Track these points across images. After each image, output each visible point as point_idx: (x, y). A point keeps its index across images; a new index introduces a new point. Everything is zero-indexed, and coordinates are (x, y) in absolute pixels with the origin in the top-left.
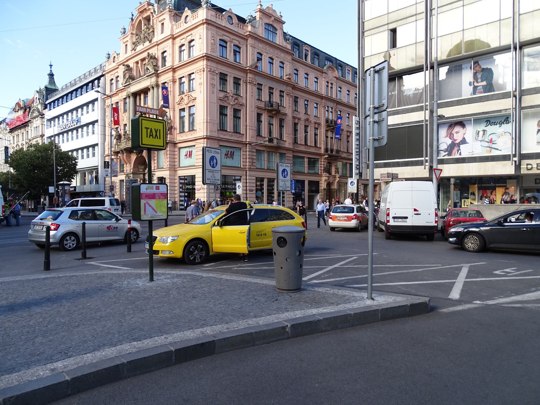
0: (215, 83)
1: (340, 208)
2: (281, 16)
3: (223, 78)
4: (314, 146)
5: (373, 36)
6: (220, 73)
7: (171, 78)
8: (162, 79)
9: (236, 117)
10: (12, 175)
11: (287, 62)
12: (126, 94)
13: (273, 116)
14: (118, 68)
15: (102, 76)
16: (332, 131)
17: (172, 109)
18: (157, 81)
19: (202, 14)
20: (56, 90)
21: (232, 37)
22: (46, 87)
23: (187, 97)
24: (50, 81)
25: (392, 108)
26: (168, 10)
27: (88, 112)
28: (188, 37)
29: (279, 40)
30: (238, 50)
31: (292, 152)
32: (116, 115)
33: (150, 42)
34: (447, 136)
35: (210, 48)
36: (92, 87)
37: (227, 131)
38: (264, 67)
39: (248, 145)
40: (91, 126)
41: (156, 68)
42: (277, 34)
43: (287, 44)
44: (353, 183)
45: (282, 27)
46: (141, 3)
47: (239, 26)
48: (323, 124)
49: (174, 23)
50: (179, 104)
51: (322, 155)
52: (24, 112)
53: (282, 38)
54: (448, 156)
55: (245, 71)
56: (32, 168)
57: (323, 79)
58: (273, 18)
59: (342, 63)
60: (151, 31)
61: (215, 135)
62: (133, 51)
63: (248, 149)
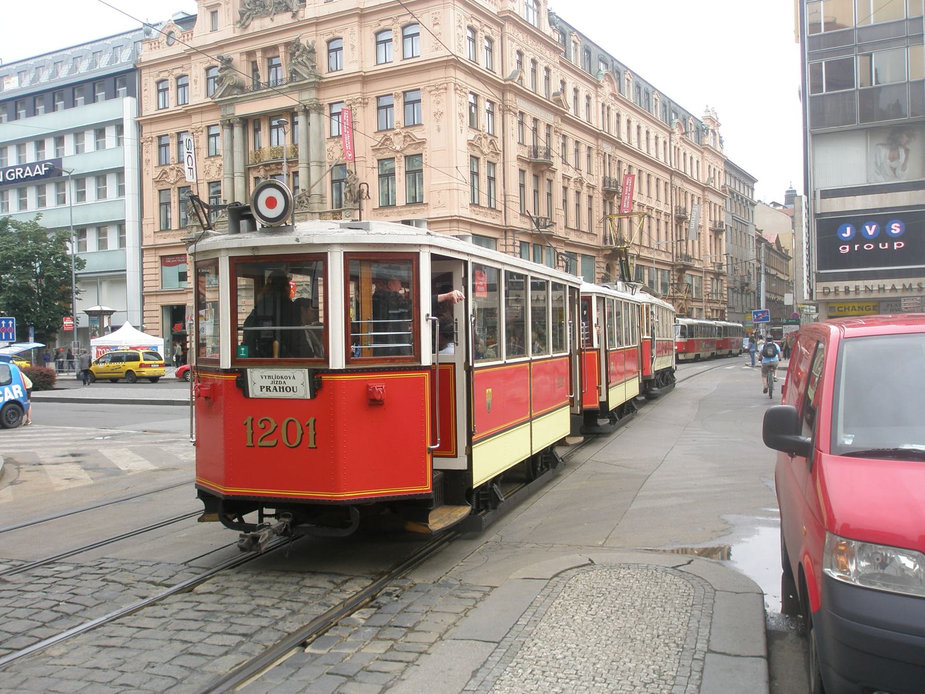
21: (485, 21)
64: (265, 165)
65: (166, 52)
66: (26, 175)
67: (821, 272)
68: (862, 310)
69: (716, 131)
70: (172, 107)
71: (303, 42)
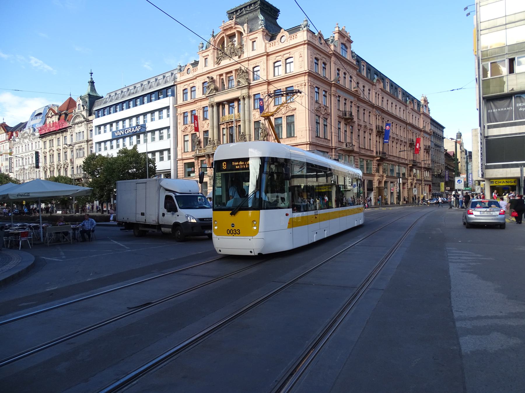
7: (266, 90)
14: (196, 78)
21: (323, 55)
22: (89, 94)
24: (91, 88)
25: (507, 121)
28: (285, 55)
29: (348, 57)
32: (196, 122)
33: (239, 57)
39: (333, 150)
44: (460, 181)
49: (267, 42)
51: (374, 157)
52: (59, 119)
57: (374, 91)
58: (346, 38)
59: (383, 76)
63: (333, 154)
64: (227, 123)
65: (187, 77)
66: (132, 131)
67: (488, 164)
68: (508, 183)
69: (427, 106)
70: (189, 100)
71: (243, 68)
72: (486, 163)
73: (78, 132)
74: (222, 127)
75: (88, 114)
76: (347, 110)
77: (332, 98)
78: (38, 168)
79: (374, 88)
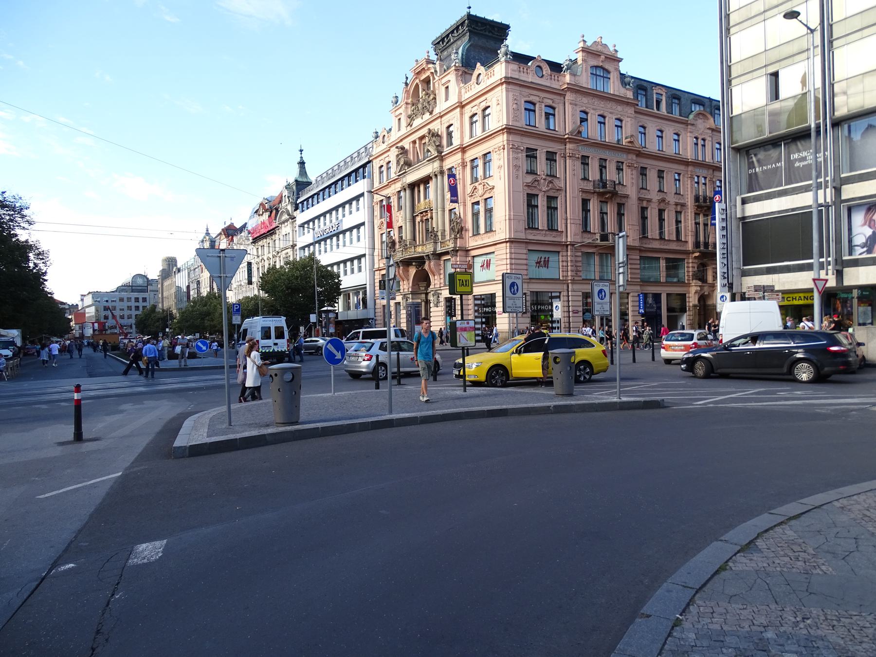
0: (520, 163)
1: (675, 335)
2: (616, 51)
3: (531, 154)
4: (675, 239)
5: (744, 85)
6: (527, 148)
7: (460, 161)
8: (448, 163)
9: (552, 209)
10: (263, 300)
11: (628, 117)
12: (400, 186)
13: (606, 200)
14: (389, 150)
15: (369, 162)
16: (707, 213)
17: (462, 204)
18: (441, 167)
19: (500, 70)
20: (310, 183)
21: (543, 95)
22: (296, 181)
23: (482, 185)
24: (300, 171)
26: (454, 68)
27: (351, 213)
29: (613, 87)
30: (551, 111)
31: (638, 252)
33: (431, 113)
34: (865, 224)
35: (511, 116)
36: (356, 178)
37: (538, 228)
38: (592, 130)
39: (569, 247)
40: (355, 231)
41: (440, 148)
42: (610, 78)
43: (625, 91)
44: (724, 298)
45: (617, 67)
46: (417, 61)
47: (553, 77)
48: (689, 204)
49: (462, 85)
50: (472, 196)
51: (690, 253)
52: (270, 216)
53: (618, 83)
54: (868, 254)
55: (563, 141)
56: (290, 291)
57: (689, 134)
58: (603, 57)
60: (431, 97)
61: (522, 236)
62: (409, 127)
63: (569, 253)
64: (421, 213)
67: (745, 267)
68: (807, 299)
72: (744, 265)
73: (284, 233)
74: (418, 219)
75: (294, 208)
76: (608, 178)
77: (568, 161)
78: (252, 284)
79: (689, 130)
